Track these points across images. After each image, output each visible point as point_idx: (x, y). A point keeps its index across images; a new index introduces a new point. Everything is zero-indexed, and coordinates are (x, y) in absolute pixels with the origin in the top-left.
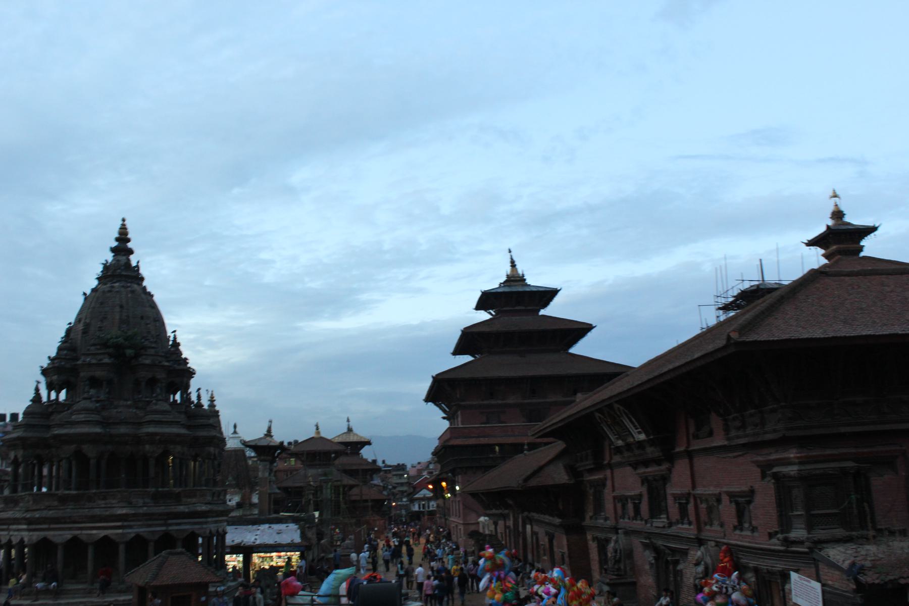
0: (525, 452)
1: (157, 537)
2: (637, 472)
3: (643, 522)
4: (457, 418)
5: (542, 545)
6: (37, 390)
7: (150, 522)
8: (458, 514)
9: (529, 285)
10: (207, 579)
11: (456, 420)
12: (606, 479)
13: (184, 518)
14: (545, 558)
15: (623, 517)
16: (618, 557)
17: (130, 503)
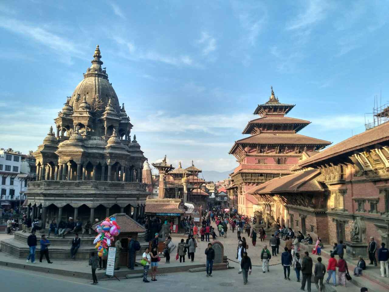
0: (280, 176)
1: (111, 206)
2: (377, 186)
3: (379, 214)
4: (245, 160)
5: (296, 220)
6: (52, 129)
7: (108, 199)
8: (243, 203)
9: (280, 103)
10: (137, 230)
11: (244, 162)
12: (347, 189)
13: (125, 197)
14: (298, 227)
15: (359, 210)
16: (357, 232)
17: (97, 188)
